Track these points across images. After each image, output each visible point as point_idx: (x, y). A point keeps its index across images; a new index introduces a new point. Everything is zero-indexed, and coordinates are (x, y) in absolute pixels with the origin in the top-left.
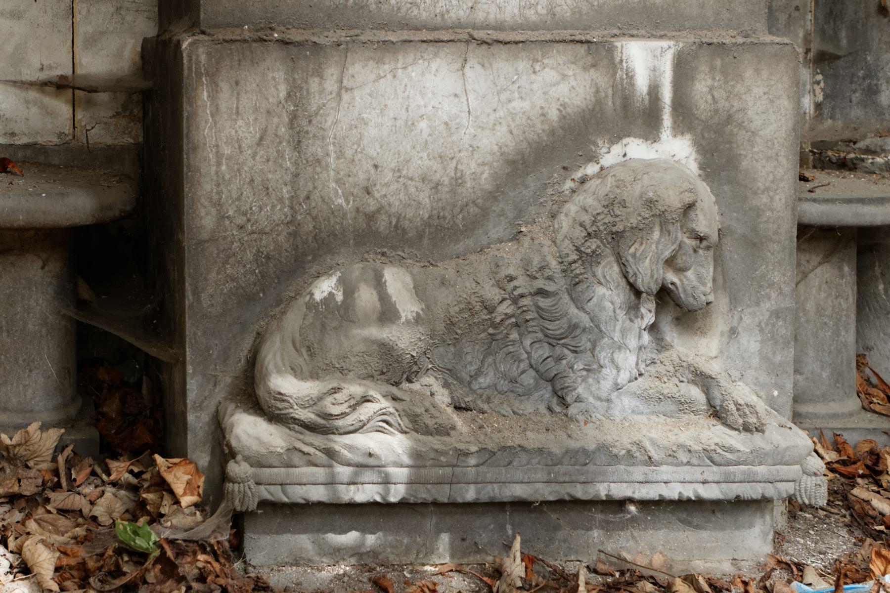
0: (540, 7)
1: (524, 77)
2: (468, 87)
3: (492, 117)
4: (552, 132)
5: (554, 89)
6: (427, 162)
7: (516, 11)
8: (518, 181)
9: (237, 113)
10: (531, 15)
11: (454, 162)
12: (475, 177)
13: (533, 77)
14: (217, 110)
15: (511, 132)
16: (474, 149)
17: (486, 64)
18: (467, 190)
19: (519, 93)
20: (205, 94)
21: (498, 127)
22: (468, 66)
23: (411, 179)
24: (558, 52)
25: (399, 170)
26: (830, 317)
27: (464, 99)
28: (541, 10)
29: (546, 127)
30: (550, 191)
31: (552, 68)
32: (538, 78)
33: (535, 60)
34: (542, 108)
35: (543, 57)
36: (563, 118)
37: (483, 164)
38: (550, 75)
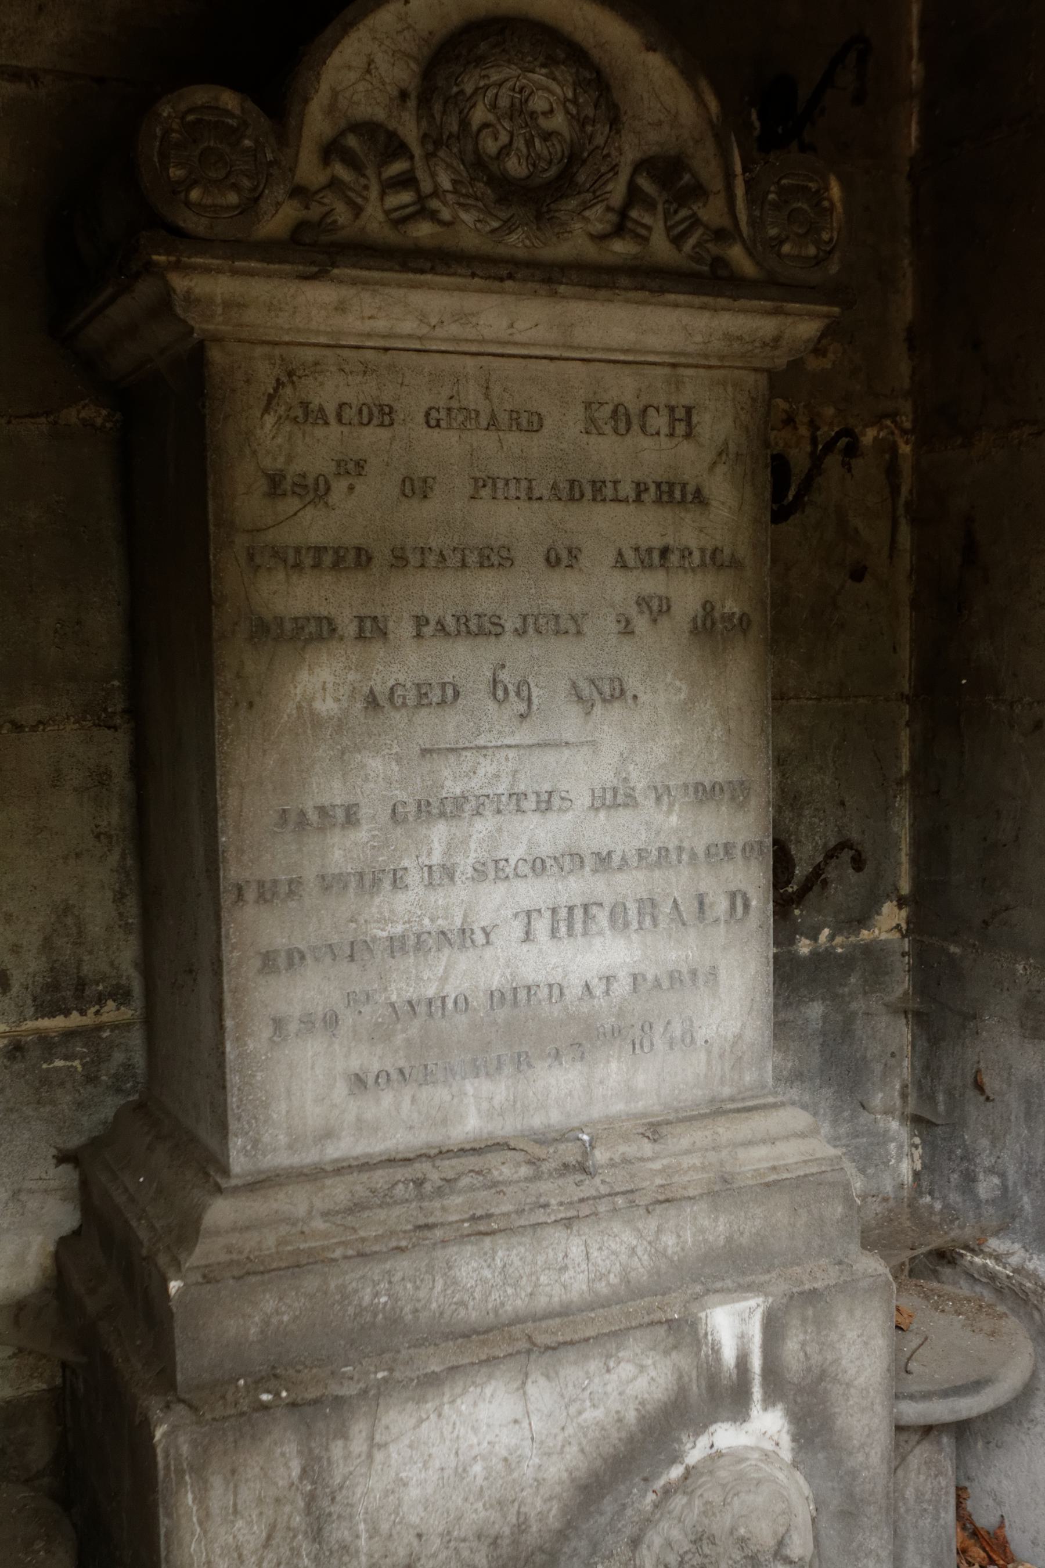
0: (612, 1276)
1: (596, 1380)
2: (531, 1408)
3: (560, 1438)
4: (631, 1439)
5: (631, 1386)
6: (483, 1514)
7: (584, 1287)
8: (592, 1509)
9: (236, 1512)
10: (602, 1288)
11: (516, 1504)
12: (542, 1516)
13: (607, 1376)
14: (208, 1515)
15: (582, 1451)
16: (539, 1482)
17: (552, 1374)
18: (532, 1538)
19: (591, 1400)
20: (190, 1496)
21: (567, 1449)
22: (530, 1381)
23: (464, 1540)
24: (635, 1339)
25: (449, 1533)
26: (930, 1501)
27: (525, 1424)
28: (613, 1279)
29: (623, 1435)
30: (629, 1512)
31: (628, 1361)
32: (613, 1377)
33: (609, 1356)
34: (618, 1412)
35: (618, 1349)
36: (641, 1418)
37: (551, 1498)
38: (626, 1370)
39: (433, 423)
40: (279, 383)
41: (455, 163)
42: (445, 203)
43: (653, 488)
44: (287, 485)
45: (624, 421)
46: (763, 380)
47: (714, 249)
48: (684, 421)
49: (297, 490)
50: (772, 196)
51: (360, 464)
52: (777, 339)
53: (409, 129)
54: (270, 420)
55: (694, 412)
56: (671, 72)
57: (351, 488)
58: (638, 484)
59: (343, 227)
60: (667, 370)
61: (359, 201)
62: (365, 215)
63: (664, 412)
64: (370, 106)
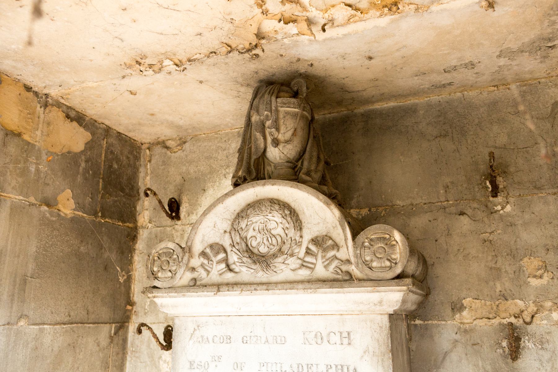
39: (245, 342)
40: (195, 330)
41: (237, 252)
42: (237, 266)
43: (334, 367)
44: (195, 365)
45: (320, 338)
46: (386, 319)
47: (344, 268)
48: (347, 337)
49: (199, 367)
50: (367, 244)
51: (220, 357)
52: (381, 302)
53: (227, 243)
54: (191, 342)
55: (352, 334)
56: (321, 204)
57: (216, 366)
58: (327, 366)
59: (204, 279)
60: (339, 316)
61: (209, 269)
62: (211, 274)
63: (339, 334)
64: (214, 238)
